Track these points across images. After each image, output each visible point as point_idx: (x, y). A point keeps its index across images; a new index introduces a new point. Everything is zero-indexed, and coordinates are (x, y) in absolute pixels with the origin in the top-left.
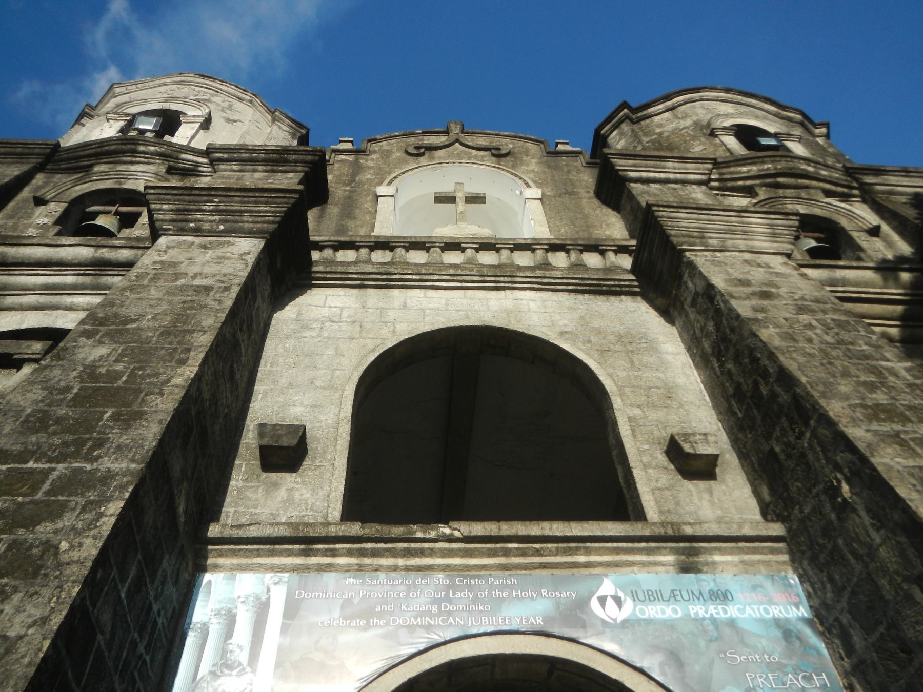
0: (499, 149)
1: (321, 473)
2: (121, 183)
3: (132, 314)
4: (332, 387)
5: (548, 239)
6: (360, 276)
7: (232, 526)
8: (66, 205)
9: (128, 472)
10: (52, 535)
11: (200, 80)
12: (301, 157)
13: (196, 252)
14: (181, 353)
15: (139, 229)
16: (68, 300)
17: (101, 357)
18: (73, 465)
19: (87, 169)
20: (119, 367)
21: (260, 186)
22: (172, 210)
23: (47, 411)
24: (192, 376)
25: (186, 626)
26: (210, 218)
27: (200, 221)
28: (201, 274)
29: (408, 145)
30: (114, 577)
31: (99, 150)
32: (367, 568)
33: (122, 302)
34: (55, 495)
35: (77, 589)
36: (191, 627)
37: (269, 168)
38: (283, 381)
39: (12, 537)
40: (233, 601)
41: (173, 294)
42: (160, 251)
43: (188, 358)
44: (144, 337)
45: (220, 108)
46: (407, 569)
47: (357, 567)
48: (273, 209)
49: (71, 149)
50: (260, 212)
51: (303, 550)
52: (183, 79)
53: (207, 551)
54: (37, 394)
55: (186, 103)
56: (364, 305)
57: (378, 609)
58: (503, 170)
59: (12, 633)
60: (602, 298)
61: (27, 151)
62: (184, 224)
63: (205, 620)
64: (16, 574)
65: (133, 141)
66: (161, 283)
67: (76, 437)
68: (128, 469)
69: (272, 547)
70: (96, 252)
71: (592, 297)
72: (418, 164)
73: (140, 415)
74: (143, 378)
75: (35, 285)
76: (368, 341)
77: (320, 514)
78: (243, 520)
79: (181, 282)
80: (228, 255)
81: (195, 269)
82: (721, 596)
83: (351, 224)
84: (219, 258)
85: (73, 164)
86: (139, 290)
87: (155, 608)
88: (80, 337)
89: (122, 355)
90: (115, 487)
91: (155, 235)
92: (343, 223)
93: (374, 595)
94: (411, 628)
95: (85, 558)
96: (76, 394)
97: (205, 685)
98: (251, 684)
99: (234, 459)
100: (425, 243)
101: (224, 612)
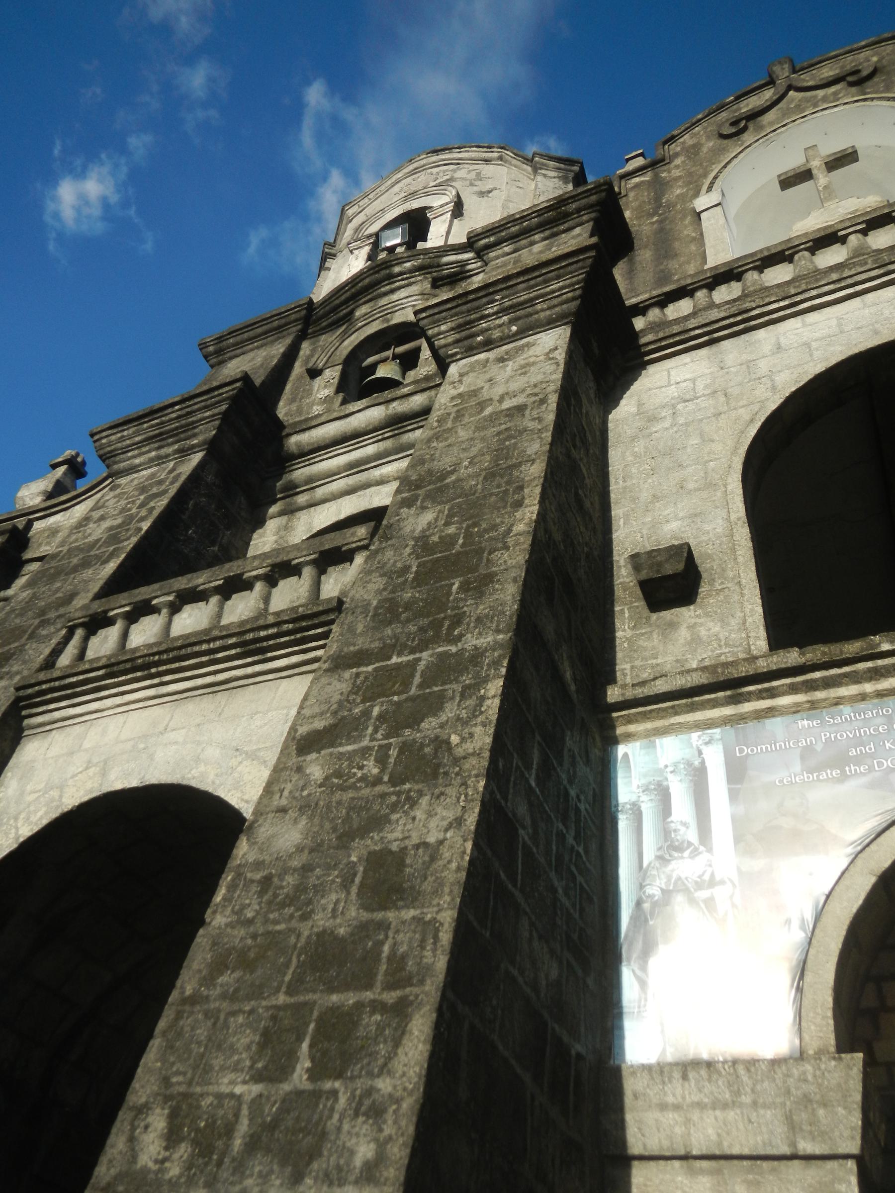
0: (857, 72)
1: (725, 597)
2: (388, 321)
3: (447, 466)
4: (710, 485)
6: (705, 329)
7: (633, 685)
8: (340, 367)
9: (495, 646)
10: (438, 730)
11: (434, 158)
12: (584, 202)
13: (494, 370)
14: (513, 494)
15: (425, 366)
16: (376, 473)
17: (429, 524)
18: (437, 650)
19: (348, 318)
20: (452, 530)
21: (544, 259)
22: (452, 329)
23: (393, 598)
24: (534, 517)
25: (613, 809)
26: (498, 322)
27: (487, 330)
28: (507, 394)
29: (720, 125)
30: (517, 764)
31: (353, 290)
32: (823, 704)
33: (432, 455)
34: (429, 687)
35: (482, 783)
36: (620, 809)
37: (547, 233)
38: (645, 496)
39: (400, 739)
40: (661, 772)
41: (484, 428)
42: (454, 383)
43: (523, 498)
44: (467, 487)
45: (468, 182)
46: (880, 694)
47: (808, 705)
48: (568, 282)
49: (326, 301)
50: (553, 292)
51: (730, 697)
52: (415, 165)
53: (611, 719)
54: (378, 582)
55: (427, 194)
56: (722, 365)
57: (853, 752)
58: (872, 99)
59: (431, 839)
61: (283, 321)
62: (470, 341)
63: (634, 798)
64: (417, 778)
65: (387, 265)
66: (466, 420)
67: (431, 619)
68: (496, 642)
69: (689, 700)
70: (387, 409)
72: (742, 145)
73: (489, 578)
74: (480, 535)
75: (339, 467)
76: (741, 411)
77: (740, 649)
78: (645, 676)
79: (488, 411)
80: (532, 360)
81: (499, 390)
84: (522, 367)
86: (445, 436)
87: (573, 793)
88: (400, 508)
89: (450, 515)
90: (488, 664)
91: (443, 366)
92: (662, 267)
93: (842, 736)
95: (481, 749)
96: (416, 572)
97: (654, 872)
98: (710, 866)
99: (613, 605)
100: (784, 251)
101: (653, 787)
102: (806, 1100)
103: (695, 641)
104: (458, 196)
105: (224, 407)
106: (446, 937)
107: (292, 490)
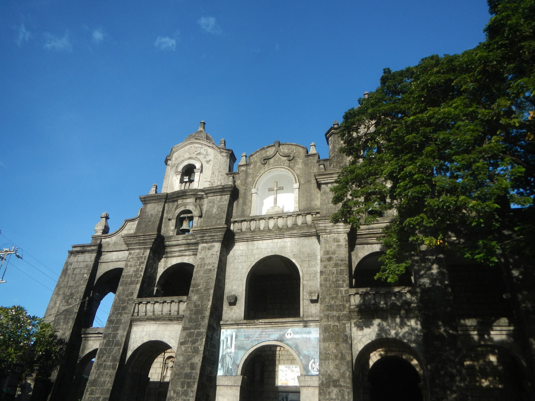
0: (290, 156)
2: (185, 207)
4: (241, 280)
45: (204, 156)
60: (307, 238)
71: (304, 238)
82: (309, 333)
83: (246, 208)
94: (255, 340)
102: (236, 380)
103: (235, 313)
105: (153, 240)
106: (198, 375)
107: (167, 252)
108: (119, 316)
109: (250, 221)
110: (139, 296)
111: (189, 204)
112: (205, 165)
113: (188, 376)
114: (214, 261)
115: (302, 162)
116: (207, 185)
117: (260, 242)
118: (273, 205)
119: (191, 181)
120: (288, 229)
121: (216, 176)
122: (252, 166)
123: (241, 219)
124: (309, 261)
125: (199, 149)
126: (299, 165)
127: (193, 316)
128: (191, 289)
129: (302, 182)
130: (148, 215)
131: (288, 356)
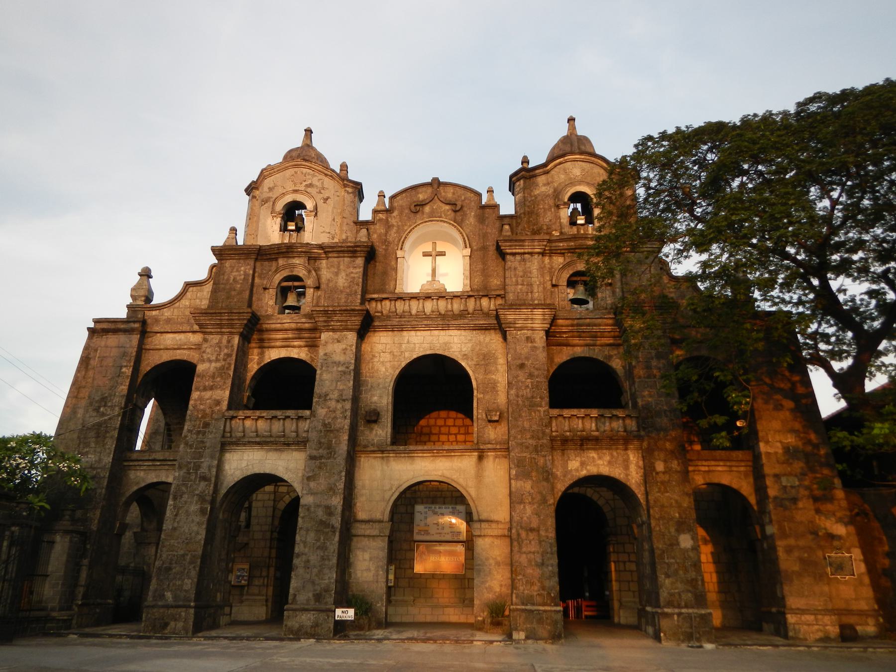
0: (456, 205)
2: (292, 272)
5: (467, 292)
11: (304, 163)
45: (318, 191)
55: (302, 194)
58: (455, 227)
60: (483, 331)
76: (396, 363)
85: (269, 257)
104: (316, 208)
105: (245, 322)
108: (201, 436)
109: (396, 300)
110: (230, 408)
111: (299, 268)
112: (320, 203)
113: (322, 523)
114: (348, 359)
115: (475, 216)
116: (324, 239)
117: (413, 333)
118: (430, 279)
119: (299, 229)
120: (456, 317)
121: (338, 224)
122: (395, 213)
123: (380, 296)
124: (487, 365)
125: (310, 176)
126: (471, 219)
127: (323, 440)
128: (315, 400)
129: (475, 248)
130: (228, 280)
131: (428, 493)
